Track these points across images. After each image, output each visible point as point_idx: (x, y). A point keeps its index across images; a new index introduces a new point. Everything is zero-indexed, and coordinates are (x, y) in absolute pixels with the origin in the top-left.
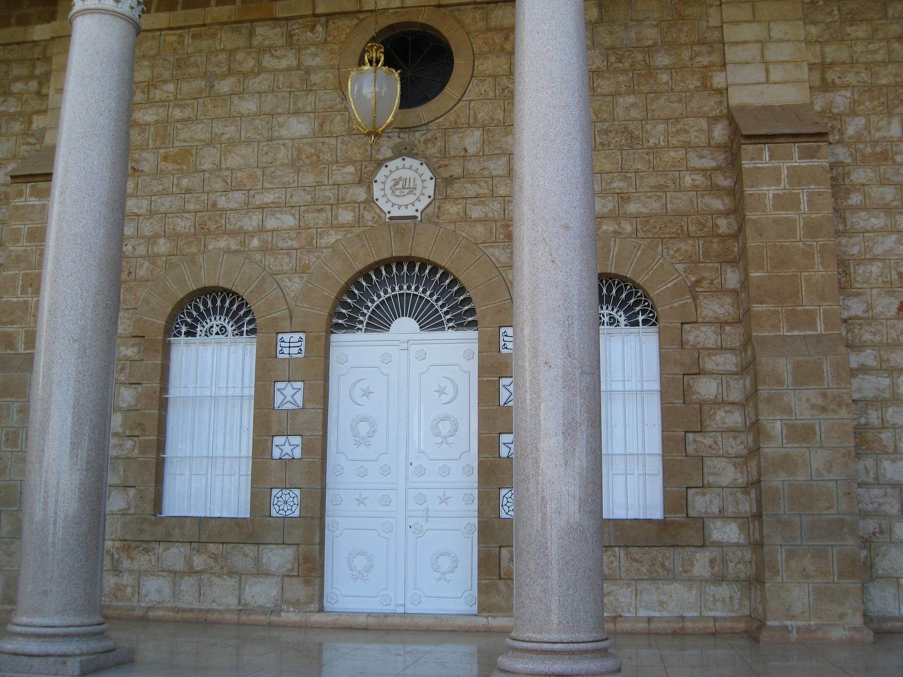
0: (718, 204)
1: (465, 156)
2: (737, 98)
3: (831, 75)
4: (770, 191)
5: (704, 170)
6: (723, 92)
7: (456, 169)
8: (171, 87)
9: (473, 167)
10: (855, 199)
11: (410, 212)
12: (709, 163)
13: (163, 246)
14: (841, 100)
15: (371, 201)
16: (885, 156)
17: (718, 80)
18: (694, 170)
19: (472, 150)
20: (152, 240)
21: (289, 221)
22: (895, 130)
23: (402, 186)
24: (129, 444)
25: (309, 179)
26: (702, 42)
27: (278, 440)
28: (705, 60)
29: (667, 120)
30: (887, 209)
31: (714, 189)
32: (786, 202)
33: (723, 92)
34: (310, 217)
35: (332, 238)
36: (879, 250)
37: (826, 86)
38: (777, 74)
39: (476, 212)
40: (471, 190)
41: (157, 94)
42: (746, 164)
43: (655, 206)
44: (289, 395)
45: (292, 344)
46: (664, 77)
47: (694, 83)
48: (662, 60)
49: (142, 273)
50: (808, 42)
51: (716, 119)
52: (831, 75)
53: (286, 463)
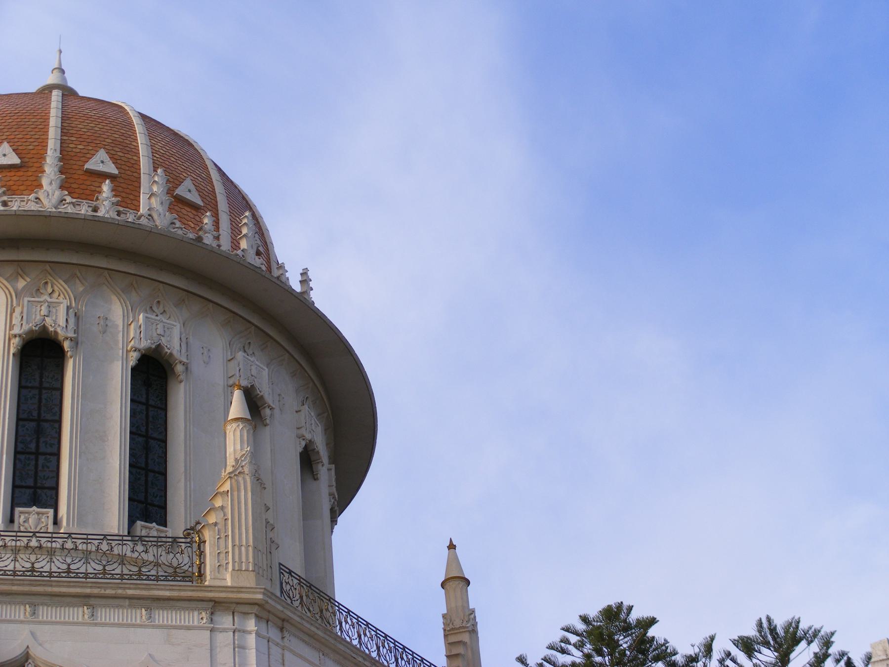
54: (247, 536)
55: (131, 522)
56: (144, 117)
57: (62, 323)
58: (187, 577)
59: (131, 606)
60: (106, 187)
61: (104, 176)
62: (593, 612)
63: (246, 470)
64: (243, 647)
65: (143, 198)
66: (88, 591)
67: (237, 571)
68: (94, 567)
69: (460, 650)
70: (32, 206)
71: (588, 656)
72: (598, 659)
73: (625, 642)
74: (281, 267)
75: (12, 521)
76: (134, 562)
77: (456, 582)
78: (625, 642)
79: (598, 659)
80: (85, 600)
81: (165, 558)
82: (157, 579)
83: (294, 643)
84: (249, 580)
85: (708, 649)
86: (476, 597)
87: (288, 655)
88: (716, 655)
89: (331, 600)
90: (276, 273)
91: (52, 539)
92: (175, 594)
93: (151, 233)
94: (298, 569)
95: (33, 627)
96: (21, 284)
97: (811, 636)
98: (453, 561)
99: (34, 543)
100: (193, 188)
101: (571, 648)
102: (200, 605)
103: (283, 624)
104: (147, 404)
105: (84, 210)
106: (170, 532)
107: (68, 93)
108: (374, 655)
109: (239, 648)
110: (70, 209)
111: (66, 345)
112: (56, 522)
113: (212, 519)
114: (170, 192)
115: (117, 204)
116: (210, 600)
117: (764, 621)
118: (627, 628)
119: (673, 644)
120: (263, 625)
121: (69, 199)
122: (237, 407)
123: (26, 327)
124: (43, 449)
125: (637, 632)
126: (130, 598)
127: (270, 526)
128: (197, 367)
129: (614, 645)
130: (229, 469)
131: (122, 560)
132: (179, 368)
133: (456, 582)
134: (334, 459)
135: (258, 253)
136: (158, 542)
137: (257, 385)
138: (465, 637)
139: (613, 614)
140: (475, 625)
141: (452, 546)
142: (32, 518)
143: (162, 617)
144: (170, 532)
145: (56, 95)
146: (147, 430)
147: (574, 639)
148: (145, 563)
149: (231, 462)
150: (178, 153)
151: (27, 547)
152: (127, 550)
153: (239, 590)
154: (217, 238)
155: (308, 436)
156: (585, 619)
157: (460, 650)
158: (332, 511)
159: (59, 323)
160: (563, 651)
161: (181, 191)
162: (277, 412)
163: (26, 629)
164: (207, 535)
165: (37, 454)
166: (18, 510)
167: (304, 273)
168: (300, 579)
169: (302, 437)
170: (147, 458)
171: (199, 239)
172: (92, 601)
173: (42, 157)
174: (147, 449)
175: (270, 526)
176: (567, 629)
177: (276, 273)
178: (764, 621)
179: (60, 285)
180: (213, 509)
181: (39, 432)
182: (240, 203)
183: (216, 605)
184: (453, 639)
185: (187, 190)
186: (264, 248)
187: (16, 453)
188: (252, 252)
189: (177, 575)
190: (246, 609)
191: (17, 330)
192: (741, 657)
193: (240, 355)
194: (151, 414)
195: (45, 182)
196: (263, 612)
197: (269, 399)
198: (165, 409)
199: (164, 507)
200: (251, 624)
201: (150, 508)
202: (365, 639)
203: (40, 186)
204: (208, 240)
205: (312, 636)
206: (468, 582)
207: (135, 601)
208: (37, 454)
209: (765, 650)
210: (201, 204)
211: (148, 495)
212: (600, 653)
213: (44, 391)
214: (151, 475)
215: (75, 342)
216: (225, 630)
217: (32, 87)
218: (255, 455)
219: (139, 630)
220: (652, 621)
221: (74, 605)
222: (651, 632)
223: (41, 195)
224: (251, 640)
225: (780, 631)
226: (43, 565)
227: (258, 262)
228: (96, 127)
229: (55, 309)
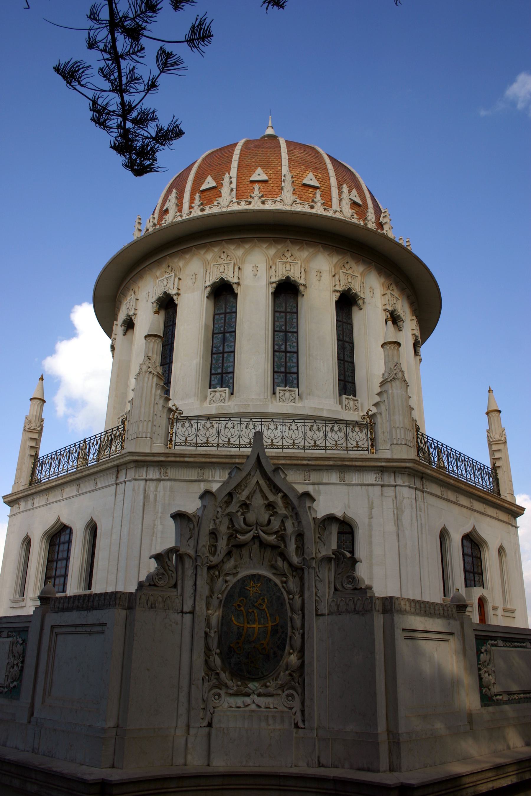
100: (357, 195)
105: (306, 209)
121: (298, 201)
146: (343, 337)
170: (344, 354)
194: (344, 327)
201: (347, 384)
213: (288, 314)
214: (346, 364)
223: (284, 198)
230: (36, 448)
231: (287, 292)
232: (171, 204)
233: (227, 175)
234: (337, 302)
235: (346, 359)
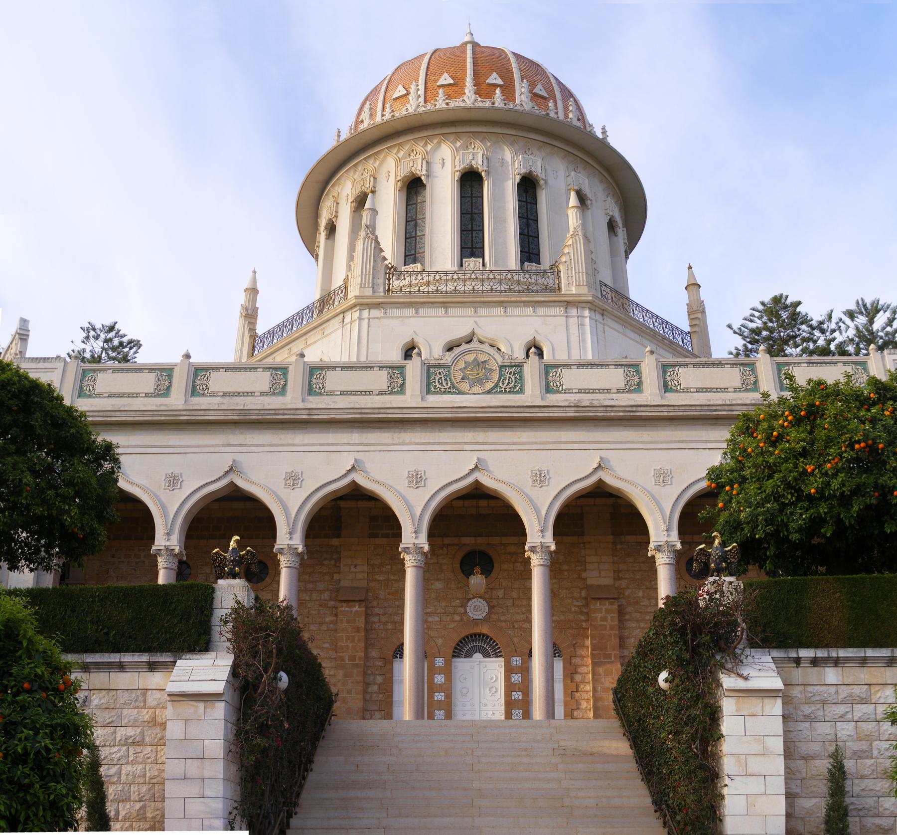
0: (583, 618)
1: (498, 598)
2: (590, 582)
3: (621, 575)
4: (599, 616)
5: (578, 606)
6: (585, 579)
7: (495, 603)
8: (389, 567)
9: (501, 602)
10: (627, 617)
11: (480, 617)
12: (580, 604)
13: (389, 626)
14: (624, 583)
15: (466, 613)
16: (637, 603)
17: (584, 575)
18: (575, 606)
19: (501, 596)
20: (385, 623)
21: (437, 619)
22: (641, 594)
23: (476, 608)
24: (381, 696)
25: (444, 604)
26: (578, 561)
27: (436, 694)
28: (579, 568)
29: (566, 588)
30: (637, 621)
31: (581, 613)
32: (604, 619)
33: (585, 579)
34: (444, 618)
35: (452, 625)
36: (634, 634)
37: (619, 579)
38: (603, 574)
39: (502, 618)
40: (500, 610)
41: (384, 569)
42: (592, 607)
43: (562, 617)
44: (439, 679)
45: (440, 662)
46: (566, 573)
47: (575, 576)
48: (565, 567)
49: (382, 635)
50: (613, 563)
51: (581, 589)
52: (621, 575)
53: (439, 702)
54: (582, 267)
55: (522, 263)
56: (514, 54)
57: (480, 163)
58: (552, 290)
59: (524, 306)
60: (498, 91)
61: (496, 86)
62: (767, 299)
63: (580, 233)
64: (583, 325)
65: (517, 95)
66: (502, 299)
67: (578, 285)
68: (504, 287)
69: (697, 322)
70: (462, 104)
71: (765, 323)
72: (770, 325)
73: (784, 315)
74: (591, 126)
75: (462, 265)
76: (525, 283)
77: (693, 286)
78: (784, 315)
79: (770, 325)
80: (501, 304)
81: (541, 281)
82: (537, 291)
83: (609, 321)
84: (584, 290)
85: (830, 317)
86: (704, 294)
87: (606, 328)
88: (835, 319)
89: (628, 299)
90: (588, 129)
91: (482, 274)
92: (547, 299)
93: (522, 113)
94: (609, 282)
95: (477, 319)
96: (458, 144)
97: (886, 308)
98: (691, 275)
99: (473, 276)
101: (756, 319)
102: (560, 304)
103: (603, 312)
104: (526, 202)
105: (487, 104)
106: (542, 267)
107: (475, 45)
108: (651, 326)
109: (581, 325)
110: (480, 104)
111: (483, 174)
112: (484, 265)
113: (563, 259)
114: (530, 91)
115: (504, 100)
116: (565, 301)
117: (860, 303)
118: (785, 307)
119: (810, 315)
120: (593, 313)
121: (479, 99)
122: (573, 200)
123: (462, 166)
124: (475, 228)
125: (791, 309)
126: (524, 302)
127: (593, 262)
128: (551, 181)
129: (778, 317)
130: (571, 233)
131: (519, 282)
132: (542, 182)
133: (693, 286)
134: (626, 224)
135: (579, 120)
136: (537, 273)
137: (583, 188)
138: (699, 315)
139: (777, 300)
140: (704, 308)
141: (690, 268)
142: (472, 263)
143: (541, 311)
144: (542, 267)
145: (469, 47)
147: (757, 314)
148: (530, 284)
149: (571, 229)
150: (533, 71)
151: (470, 278)
152: (521, 277)
153: (579, 295)
154: (557, 113)
155: (611, 214)
156: (763, 304)
157: (697, 322)
158: (626, 252)
159: (479, 164)
160: (752, 321)
161: (536, 90)
162: (594, 201)
163: (472, 320)
164: (561, 267)
165: (472, 230)
166: (464, 260)
167: (604, 128)
168: (611, 288)
169: (608, 214)
171: (548, 114)
172: (505, 304)
173: (464, 79)
174: (528, 225)
175: (593, 262)
176: (753, 309)
177: (588, 129)
178: (860, 303)
179: (478, 143)
180: (564, 254)
181: (472, 219)
182: (567, 94)
183: (568, 304)
184: (692, 316)
185: (540, 90)
186: (581, 117)
187: (462, 231)
188: (576, 119)
189: (547, 289)
190: (584, 305)
191: (458, 168)
192: (848, 320)
193: (573, 173)
195: (467, 91)
196: (592, 306)
197: (589, 195)
198: (536, 204)
199: (538, 255)
200: (587, 313)
202: (646, 318)
203: (465, 93)
204: (552, 114)
205: (619, 318)
206: (699, 286)
207: (526, 304)
208: (472, 230)
209: (860, 316)
210: (546, 95)
211: (530, 250)
212: (771, 321)
214: (531, 238)
215: (488, 172)
216: (573, 317)
217: (457, 43)
218: (584, 225)
219: (530, 318)
220: (799, 303)
221: (495, 307)
222: (798, 309)
223: (465, 98)
224: (587, 321)
225: (869, 306)
226: (479, 287)
227: (578, 124)
228: (490, 63)
229: (476, 155)
230: (252, 330)
231: (470, 181)
232: (365, 115)
233: (414, 83)
234: (519, 185)
235: (530, 233)
